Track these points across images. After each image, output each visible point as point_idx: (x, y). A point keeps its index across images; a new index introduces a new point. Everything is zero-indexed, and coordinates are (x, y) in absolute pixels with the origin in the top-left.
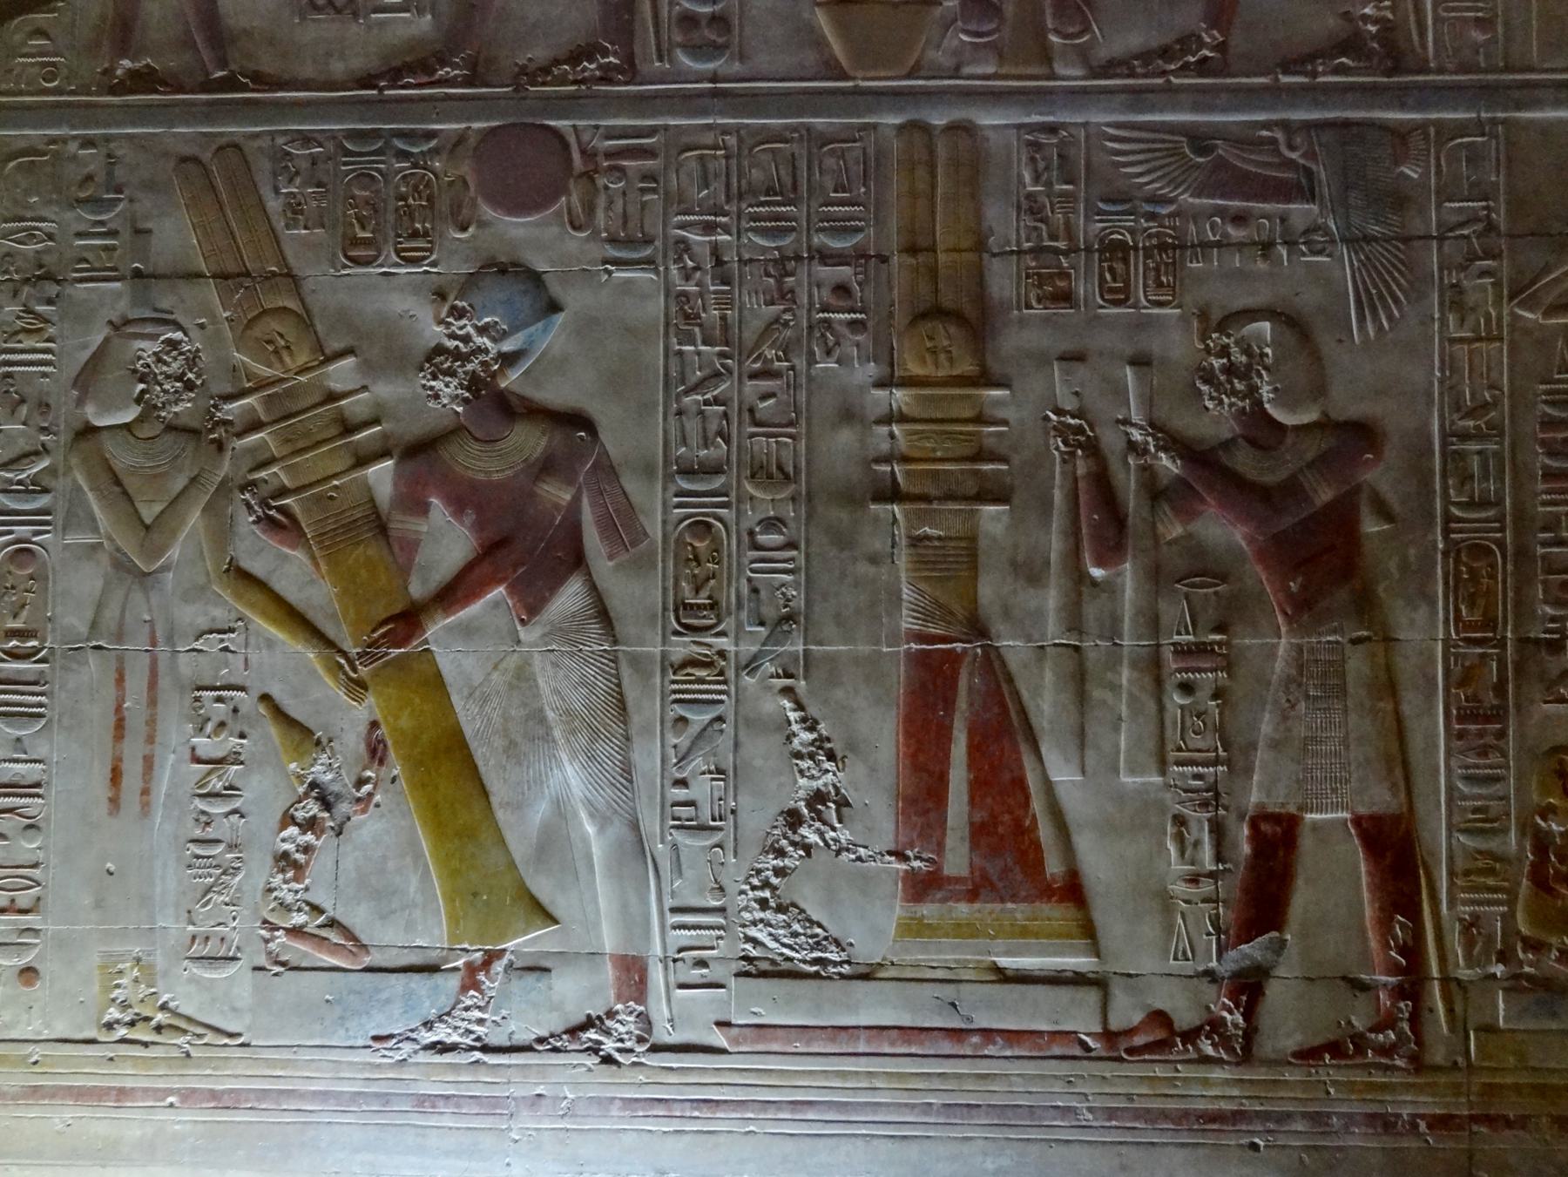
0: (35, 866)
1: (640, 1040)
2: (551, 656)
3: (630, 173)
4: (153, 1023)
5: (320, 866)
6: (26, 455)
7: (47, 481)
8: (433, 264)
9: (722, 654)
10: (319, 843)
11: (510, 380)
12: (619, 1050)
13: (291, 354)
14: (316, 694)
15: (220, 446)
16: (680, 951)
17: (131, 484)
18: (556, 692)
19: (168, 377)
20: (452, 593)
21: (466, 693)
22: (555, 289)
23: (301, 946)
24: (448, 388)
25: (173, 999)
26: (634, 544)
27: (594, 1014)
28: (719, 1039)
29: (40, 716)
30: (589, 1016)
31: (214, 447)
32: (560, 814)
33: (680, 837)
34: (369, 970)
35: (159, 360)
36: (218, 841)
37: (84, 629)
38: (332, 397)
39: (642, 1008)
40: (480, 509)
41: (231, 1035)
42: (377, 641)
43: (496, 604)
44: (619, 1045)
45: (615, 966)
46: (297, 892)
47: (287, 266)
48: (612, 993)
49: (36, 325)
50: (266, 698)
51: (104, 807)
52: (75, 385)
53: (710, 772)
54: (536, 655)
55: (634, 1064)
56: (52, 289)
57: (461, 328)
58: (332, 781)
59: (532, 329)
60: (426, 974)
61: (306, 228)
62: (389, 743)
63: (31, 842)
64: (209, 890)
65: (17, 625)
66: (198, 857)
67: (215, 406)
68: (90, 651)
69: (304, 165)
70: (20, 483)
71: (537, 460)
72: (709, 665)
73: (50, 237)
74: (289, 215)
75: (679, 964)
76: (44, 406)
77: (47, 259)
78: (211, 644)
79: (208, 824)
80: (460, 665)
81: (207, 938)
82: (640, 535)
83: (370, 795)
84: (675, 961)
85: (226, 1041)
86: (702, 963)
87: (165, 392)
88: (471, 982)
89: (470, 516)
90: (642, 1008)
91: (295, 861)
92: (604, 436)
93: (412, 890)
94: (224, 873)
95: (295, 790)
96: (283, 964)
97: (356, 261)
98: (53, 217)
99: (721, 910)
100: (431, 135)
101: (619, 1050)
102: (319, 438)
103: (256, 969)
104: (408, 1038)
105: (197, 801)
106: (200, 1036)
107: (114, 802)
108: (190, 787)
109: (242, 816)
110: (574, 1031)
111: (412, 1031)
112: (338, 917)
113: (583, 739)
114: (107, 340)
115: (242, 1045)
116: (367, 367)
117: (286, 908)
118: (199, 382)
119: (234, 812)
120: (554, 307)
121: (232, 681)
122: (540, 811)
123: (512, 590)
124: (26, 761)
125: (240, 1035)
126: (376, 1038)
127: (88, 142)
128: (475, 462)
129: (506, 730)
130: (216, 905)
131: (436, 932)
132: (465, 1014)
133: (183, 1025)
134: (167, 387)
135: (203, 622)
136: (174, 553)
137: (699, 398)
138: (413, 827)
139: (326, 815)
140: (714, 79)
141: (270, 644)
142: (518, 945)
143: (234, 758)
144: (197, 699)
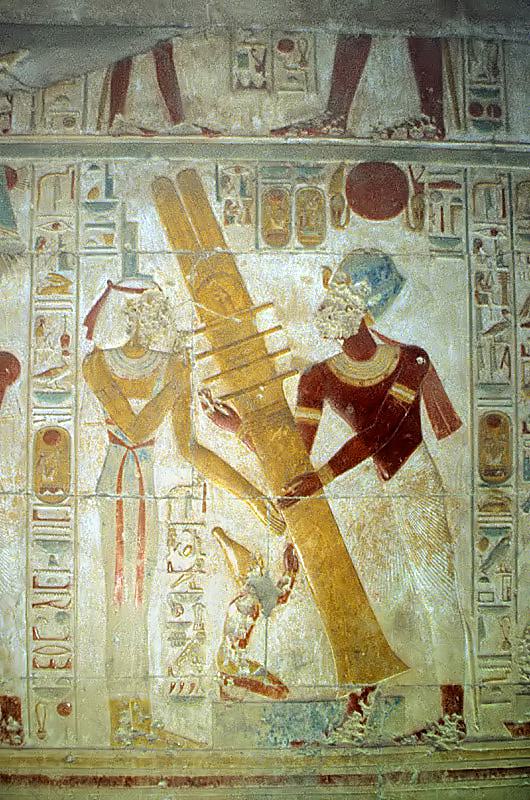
1: (460, 738)
20: (342, 462)
44: (447, 739)
45: (444, 692)
49: (59, 285)
50: (217, 529)
57: (341, 289)
61: (240, 222)
89: (350, 409)
101: (447, 743)
110: (418, 734)
113: (425, 552)
127: (94, 167)
136: (156, 434)
140: (493, 141)
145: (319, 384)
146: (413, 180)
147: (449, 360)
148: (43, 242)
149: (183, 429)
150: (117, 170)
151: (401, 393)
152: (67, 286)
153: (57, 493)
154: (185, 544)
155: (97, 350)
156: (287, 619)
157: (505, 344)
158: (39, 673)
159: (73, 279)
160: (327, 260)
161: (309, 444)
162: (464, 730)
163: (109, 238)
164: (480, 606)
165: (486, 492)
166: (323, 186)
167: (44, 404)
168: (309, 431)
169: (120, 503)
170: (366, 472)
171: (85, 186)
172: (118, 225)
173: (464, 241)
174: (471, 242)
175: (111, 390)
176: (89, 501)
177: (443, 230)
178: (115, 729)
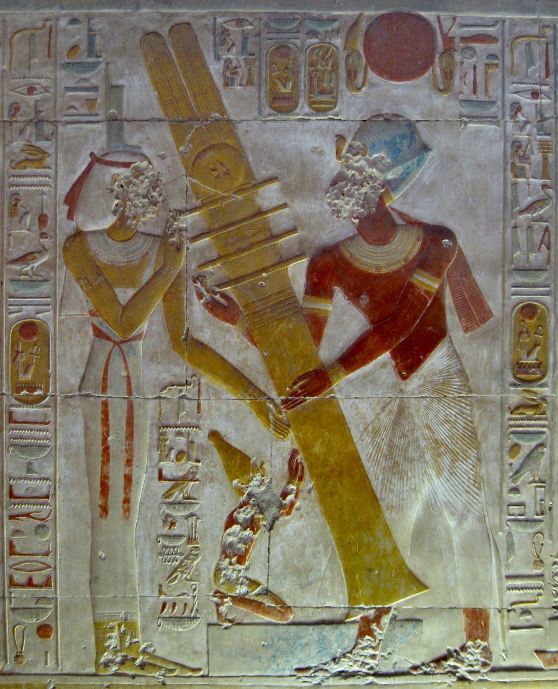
1: (485, 665)
2: (425, 402)
3: (478, 52)
4: (138, 662)
5: (257, 553)
9: (544, 399)
10: (256, 536)
12: (470, 672)
16: (512, 604)
20: (354, 357)
21: (361, 427)
23: (243, 609)
25: (151, 646)
26: (484, 320)
27: (451, 648)
28: (537, 662)
30: (449, 651)
31: (174, 248)
33: (514, 528)
36: (180, 536)
39: (484, 644)
40: (372, 294)
41: (194, 670)
43: (384, 365)
44: (470, 668)
45: (467, 616)
46: (240, 571)
48: (464, 635)
49: (35, 157)
51: (98, 511)
53: (535, 482)
55: (480, 680)
57: (357, 161)
58: (264, 492)
59: (410, 163)
60: (334, 626)
61: (241, 85)
62: (305, 466)
64: (175, 570)
66: (167, 547)
67: (172, 217)
69: (240, 38)
71: (415, 259)
72: (536, 407)
74: (228, 74)
75: (512, 613)
80: (357, 408)
81: (174, 605)
84: (509, 611)
85: (190, 674)
86: (526, 612)
87: (136, 206)
88: (366, 629)
89: (365, 300)
90: (484, 644)
92: (460, 242)
93: (323, 568)
96: (230, 621)
97: (280, 111)
99: (541, 576)
100: (333, 20)
101: (470, 672)
104: (322, 669)
105: (164, 507)
106: (171, 671)
110: (438, 661)
111: (325, 664)
112: (271, 589)
113: (446, 461)
115: (202, 676)
116: (286, 190)
118: (160, 199)
119: (192, 515)
120: (426, 148)
122: (415, 512)
124: (37, 479)
125: (200, 670)
126: (299, 670)
127: (74, 21)
132: (364, 652)
133: (159, 663)
135: (167, 377)
136: (144, 327)
137: (529, 215)
139: (261, 516)
142: (400, 603)
145: (330, 270)
146: (442, 31)
147: (476, 241)
148: (17, 109)
149: (175, 319)
150: (98, 25)
151: (425, 282)
152: (42, 159)
153: (36, 393)
155: (79, 234)
156: (291, 533)
157: (545, 224)
158: (16, 592)
159: (51, 151)
160: (340, 127)
161: (318, 336)
162: (490, 658)
163: (91, 103)
164: (509, 520)
165: (518, 393)
166: (338, 42)
167: (22, 292)
168: (317, 324)
169: (105, 405)
171: (63, 42)
172: (102, 91)
173: (499, 103)
174: (508, 105)
175: (95, 277)
176: (72, 402)
177: (475, 92)
178: (99, 654)
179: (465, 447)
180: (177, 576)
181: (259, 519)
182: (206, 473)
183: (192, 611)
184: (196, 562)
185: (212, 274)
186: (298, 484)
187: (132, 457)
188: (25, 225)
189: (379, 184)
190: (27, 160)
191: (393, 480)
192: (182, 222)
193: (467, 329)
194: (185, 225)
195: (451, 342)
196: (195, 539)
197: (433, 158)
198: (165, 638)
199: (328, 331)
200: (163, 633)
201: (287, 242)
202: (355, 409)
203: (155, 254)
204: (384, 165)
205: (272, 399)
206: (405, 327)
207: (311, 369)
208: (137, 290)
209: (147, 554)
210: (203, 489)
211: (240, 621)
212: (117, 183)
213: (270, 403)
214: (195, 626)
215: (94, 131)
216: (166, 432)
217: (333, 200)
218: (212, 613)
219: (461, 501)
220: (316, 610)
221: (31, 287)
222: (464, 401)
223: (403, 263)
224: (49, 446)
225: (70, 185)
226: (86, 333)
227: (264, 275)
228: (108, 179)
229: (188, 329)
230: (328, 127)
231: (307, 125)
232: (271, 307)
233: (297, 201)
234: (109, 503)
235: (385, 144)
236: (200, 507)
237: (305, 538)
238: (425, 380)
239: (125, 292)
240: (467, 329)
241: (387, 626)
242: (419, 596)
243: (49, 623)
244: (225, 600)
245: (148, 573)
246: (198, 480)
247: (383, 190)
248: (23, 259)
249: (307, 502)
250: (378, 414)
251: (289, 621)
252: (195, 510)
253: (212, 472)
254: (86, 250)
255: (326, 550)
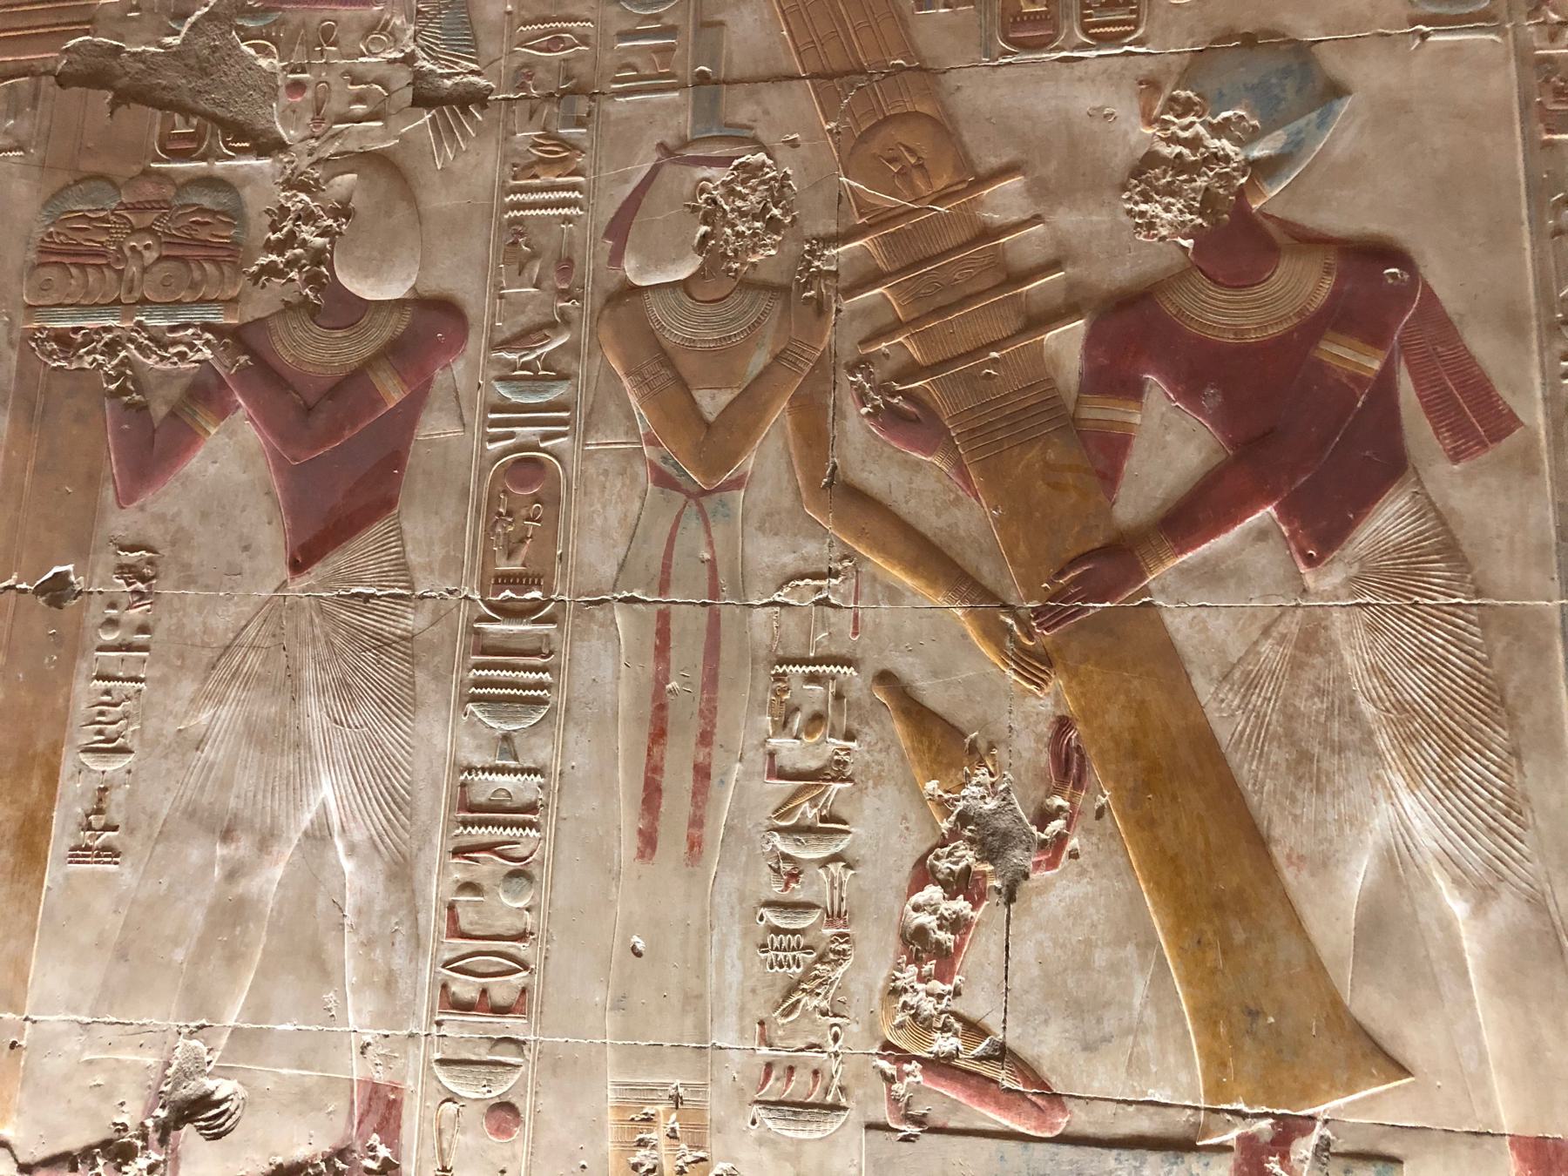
0: (521, 936)
5: (981, 953)
6: (539, 328)
7: (565, 363)
8: (1140, 42)
10: (977, 915)
11: (1268, 198)
13: (927, 177)
14: (967, 671)
15: (820, 308)
17: (688, 365)
18: (1376, 671)
19: (742, 214)
20: (1190, 517)
22: (1334, 64)
23: (951, 1091)
24: (1166, 214)
26: (1497, 435)
29: (541, 702)
31: (810, 310)
32: (1398, 879)
34: (1063, 1139)
35: (731, 193)
36: (808, 906)
37: (609, 570)
38: (988, 233)
42: (1064, 589)
43: (1262, 534)
47: (918, 56)
49: (559, 155)
50: (885, 678)
52: (607, 235)
54: (1336, 614)
56: (582, 105)
58: (994, 812)
59: (1302, 122)
61: (946, 6)
62: (1091, 753)
63: (516, 896)
64: (793, 988)
65: (515, 566)
66: (777, 931)
67: (809, 252)
68: (616, 605)
70: (525, 366)
73: (584, 40)
76: (566, 265)
77: (581, 69)
78: (801, 595)
79: (794, 877)
80: (1205, 629)
81: (791, 1069)
82: (1500, 422)
83: (1061, 839)
87: (740, 235)
89: (1212, 397)
91: (938, 943)
93: (1137, 1002)
94: (821, 959)
95: (935, 826)
96: (918, 1121)
98: (587, 14)
102: (969, 290)
103: (870, 1127)
105: (777, 839)
107: (648, 841)
108: (765, 816)
109: (848, 866)
112: (1011, 1043)
114: (655, 170)
116: (1040, 190)
117: (923, 1024)
119: (835, 858)
120: (1336, 90)
121: (834, 650)
122: (1358, 874)
123: (1285, 512)
124: (515, 771)
128: (1224, 315)
129: (1290, 734)
130: (805, 1013)
131: (1184, 1078)
134: (741, 228)
135: (790, 561)
136: (748, 462)
138: (1136, 897)
139: (989, 868)
141: (894, 594)
142: (1338, 1110)
143: (835, 771)
144: (779, 677)
153: (528, 596)
154: (807, 710)
160: (1148, 66)
161: (1110, 478)
168: (1108, 453)
169: (664, 617)
170: (1252, 536)
179: (1475, 721)
180: (798, 1001)
181: (984, 874)
182: (867, 765)
183: (827, 1091)
184: (841, 970)
185: (886, 356)
186: (1072, 795)
187: (714, 726)
188: (531, 278)
189: (1234, 169)
190: (542, 161)
191: (1299, 795)
192: (829, 261)
193: (1457, 454)
194: (833, 268)
195: (1419, 482)
196: (839, 915)
197: (1352, 112)
198: (765, 1155)
199: (1133, 464)
200: (761, 1142)
201: (1040, 287)
202: (1200, 632)
203: (774, 322)
204: (1244, 130)
205: (1012, 607)
206: (1310, 444)
207: (1097, 545)
208: (737, 392)
209: (735, 944)
210: (860, 799)
211: (939, 1123)
212: (704, 196)
213: (1008, 615)
214: (836, 1126)
215: (665, 105)
216: (784, 674)
217: (1136, 203)
218: (875, 1099)
219: (1476, 851)
220: (1121, 1109)
221: (535, 392)
222: (1461, 613)
223: (1296, 321)
224: (547, 703)
225: (618, 205)
226: (634, 479)
227: (994, 354)
228: (688, 188)
229: (835, 467)
230: (1123, 68)
231: (1079, 69)
232: (1006, 418)
233: (1061, 210)
234: (662, 829)
235: (1247, 89)
236: (853, 841)
237: (1093, 925)
238: (1362, 566)
239: (713, 398)
240: (1457, 454)
241: (1306, 1167)
242: (1388, 1091)
243: (513, 1100)
244: (907, 1067)
245: (734, 992)
246: (849, 780)
247: (1243, 180)
248: (522, 338)
249: (1094, 839)
250: (1256, 643)
251: (1057, 1133)
252: (841, 847)
253: (880, 764)
254: (642, 319)
255: (1143, 956)
